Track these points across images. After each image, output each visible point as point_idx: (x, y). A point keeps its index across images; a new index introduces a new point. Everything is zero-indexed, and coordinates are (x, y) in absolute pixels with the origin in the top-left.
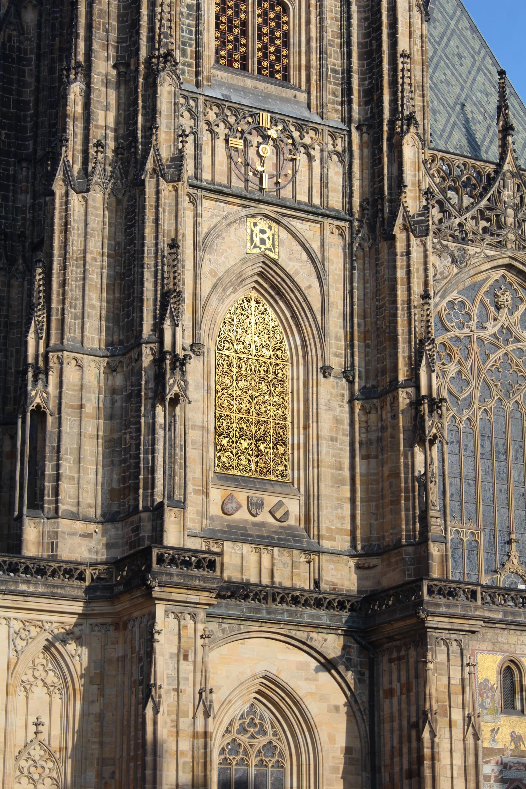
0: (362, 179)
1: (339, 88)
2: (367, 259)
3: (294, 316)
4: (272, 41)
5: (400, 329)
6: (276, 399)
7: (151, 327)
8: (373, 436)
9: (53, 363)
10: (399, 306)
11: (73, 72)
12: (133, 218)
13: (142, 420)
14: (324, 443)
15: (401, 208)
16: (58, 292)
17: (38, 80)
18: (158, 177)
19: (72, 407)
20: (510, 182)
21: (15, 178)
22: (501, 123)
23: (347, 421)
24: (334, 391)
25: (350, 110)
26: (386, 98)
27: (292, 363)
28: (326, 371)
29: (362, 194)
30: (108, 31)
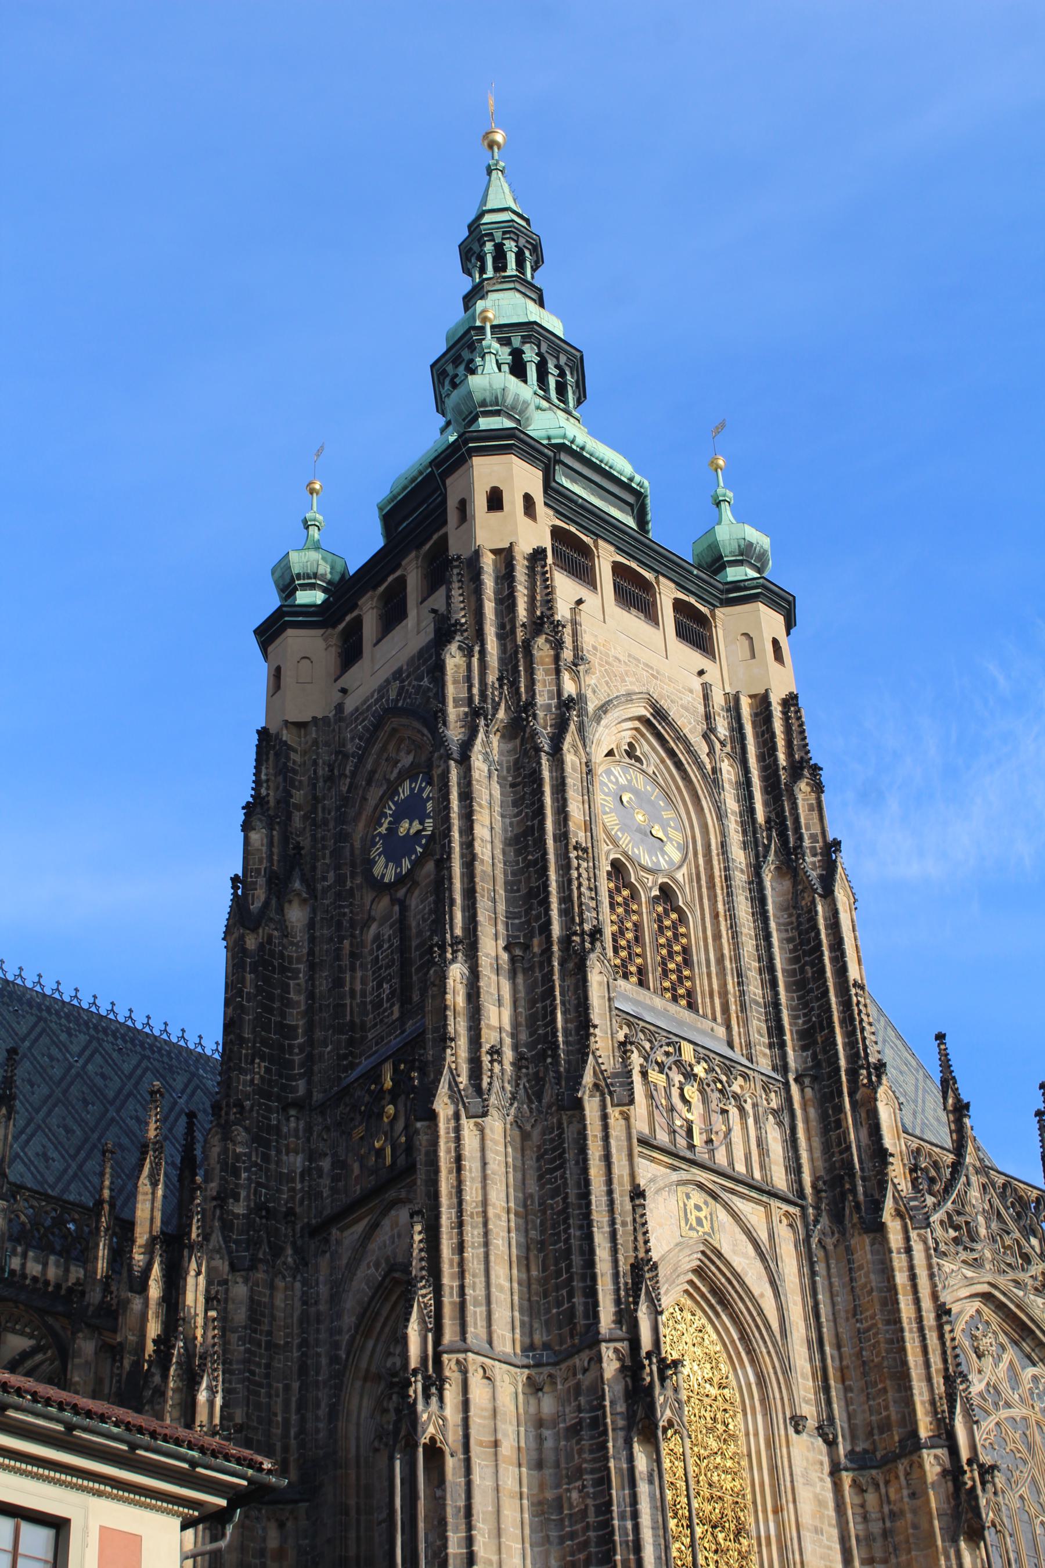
0: (810, 1150)
1: (764, 1026)
2: (833, 1262)
3: (744, 1337)
4: (671, 954)
5: (911, 1359)
6: (729, 1463)
7: (612, 1318)
8: (876, 1528)
9: (450, 1370)
10: (905, 1325)
11: (449, 950)
12: (561, 1156)
13: (612, 1464)
14: (806, 1535)
15: (890, 1186)
16: (451, 1261)
17: (311, 996)
18: (602, 1095)
19: (480, 1444)
20: (973, 1179)
21: (278, 1129)
22: (950, 1101)
23: (831, 1504)
24: (811, 1455)
25: (784, 1056)
26: (839, 1040)
27: (744, 1411)
28: (797, 1423)
29: (813, 1170)
30: (494, 901)
